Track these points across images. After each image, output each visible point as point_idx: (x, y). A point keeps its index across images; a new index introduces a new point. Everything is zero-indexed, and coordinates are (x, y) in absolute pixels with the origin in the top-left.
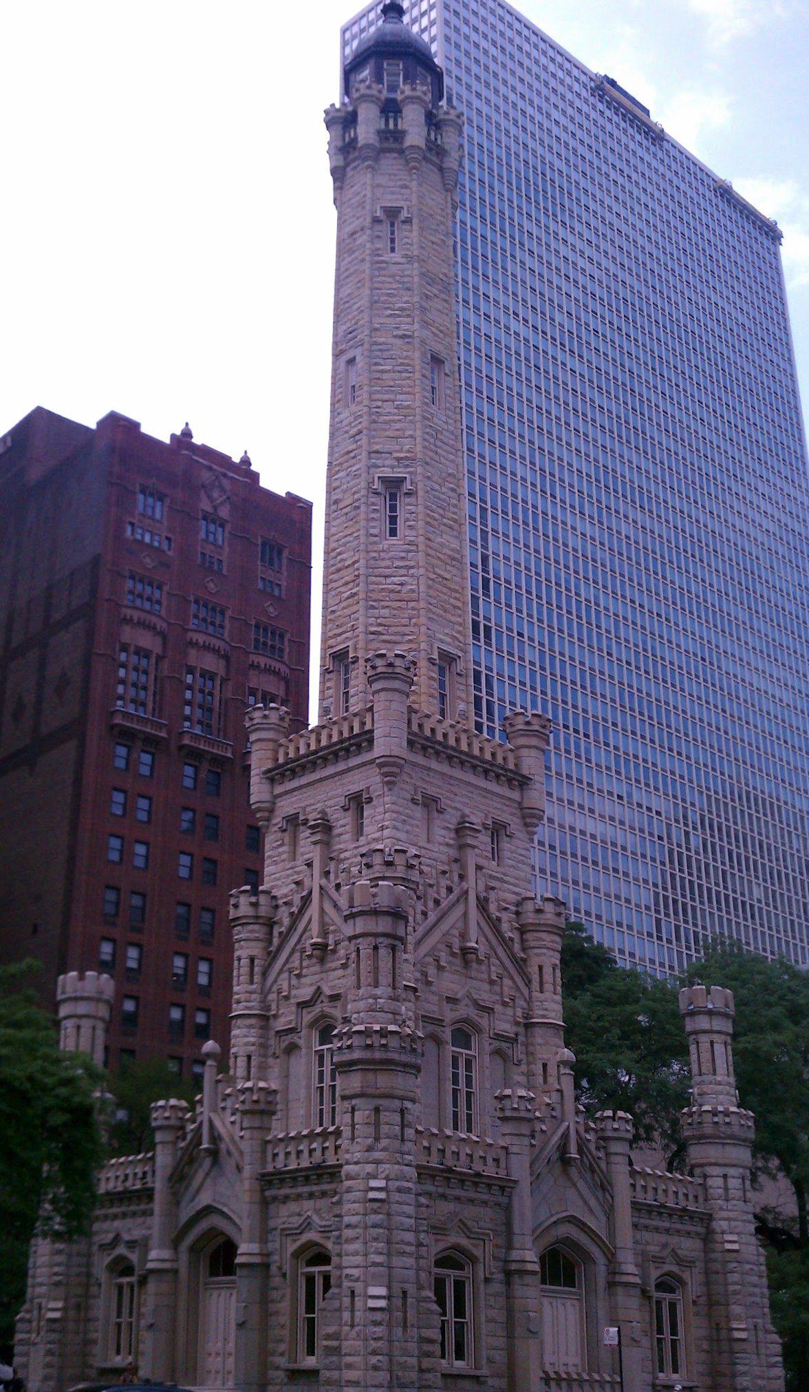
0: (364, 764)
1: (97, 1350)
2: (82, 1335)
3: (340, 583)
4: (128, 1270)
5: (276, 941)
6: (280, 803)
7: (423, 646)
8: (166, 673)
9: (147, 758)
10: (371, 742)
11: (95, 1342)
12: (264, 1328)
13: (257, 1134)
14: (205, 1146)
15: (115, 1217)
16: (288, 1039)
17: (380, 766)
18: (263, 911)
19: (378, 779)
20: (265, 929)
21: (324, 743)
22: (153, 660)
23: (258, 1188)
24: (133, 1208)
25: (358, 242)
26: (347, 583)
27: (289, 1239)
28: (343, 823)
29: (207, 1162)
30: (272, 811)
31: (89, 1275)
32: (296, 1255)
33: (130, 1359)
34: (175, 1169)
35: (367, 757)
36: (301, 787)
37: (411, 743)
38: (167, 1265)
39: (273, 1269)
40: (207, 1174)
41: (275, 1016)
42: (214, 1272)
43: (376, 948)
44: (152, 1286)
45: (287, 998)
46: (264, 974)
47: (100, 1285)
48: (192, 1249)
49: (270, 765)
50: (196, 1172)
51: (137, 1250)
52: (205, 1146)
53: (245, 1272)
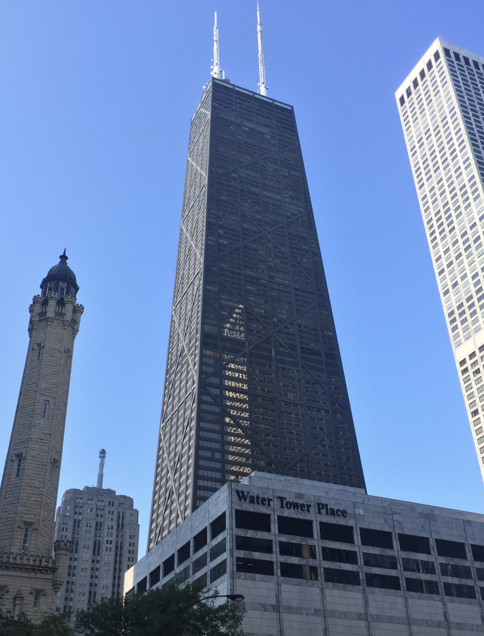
0: (44, 579)
3: (31, 492)
19: (51, 587)
25: (55, 354)
26: (35, 494)
28: (29, 599)
36: (7, 575)
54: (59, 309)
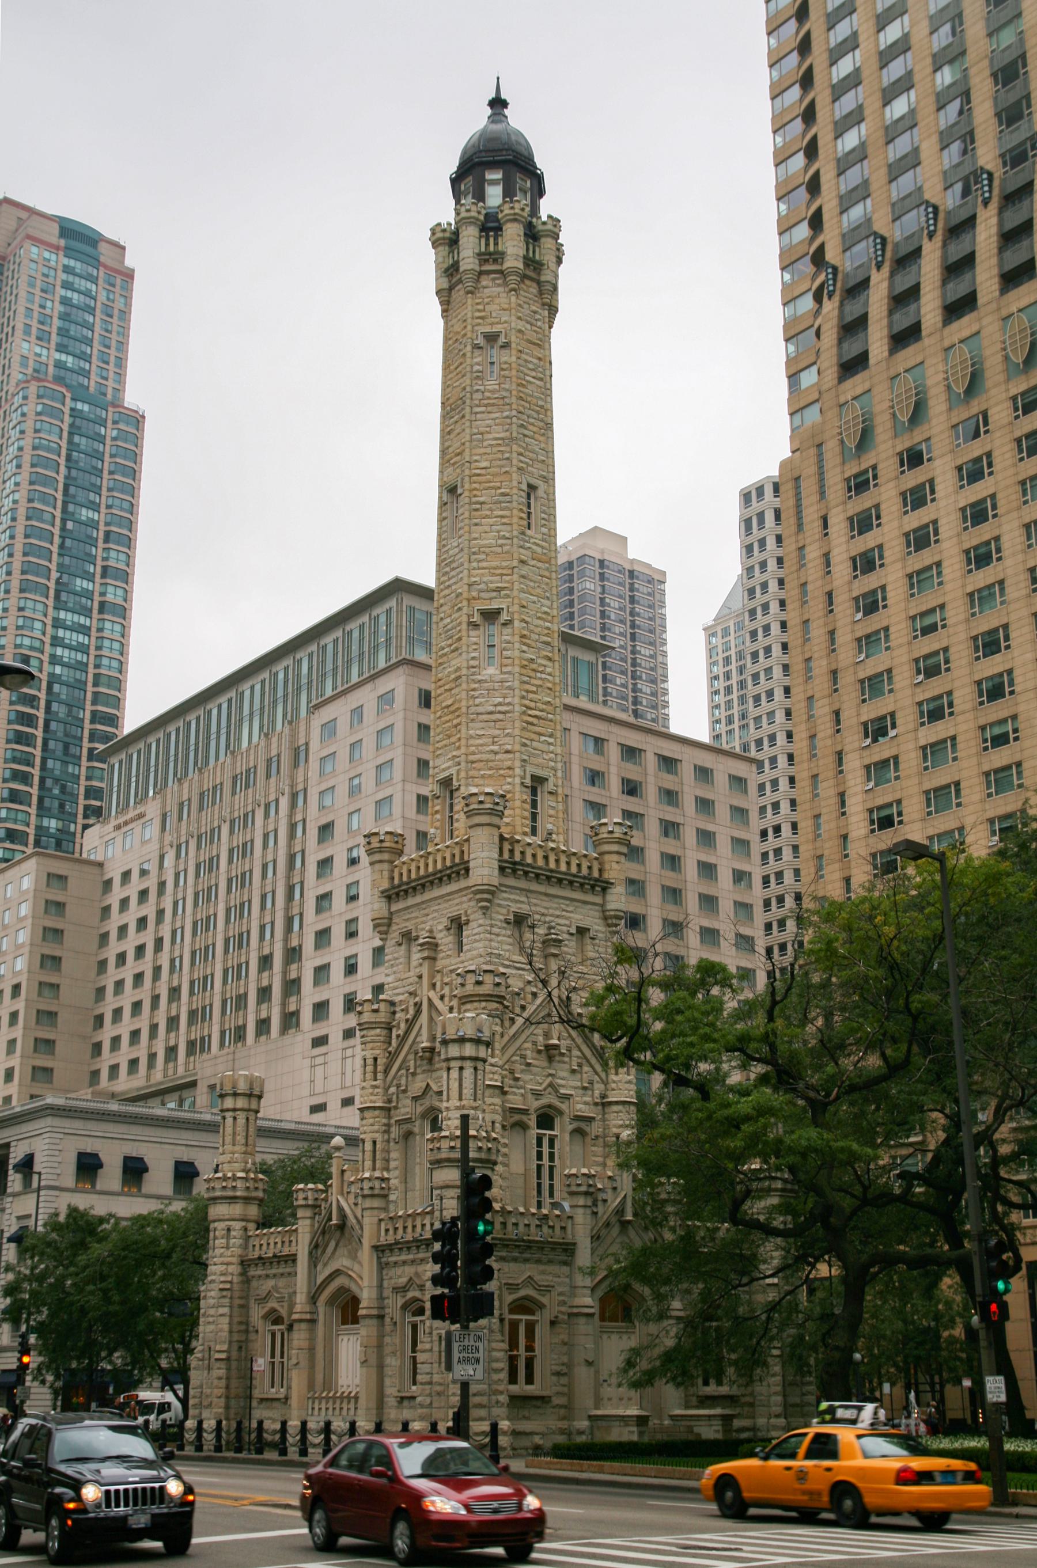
4: (278, 1320)
5: (394, 1043)
6: (395, 920)
7: (518, 771)
10: (467, 870)
12: (381, 1367)
14: (334, 1222)
16: (405, 1127)
17: (476, 893)
18: (382, 1017)
20: (384, 1032)
21: (430, 869)
28: (446, 940)
29: (338, 1234)
30: (389, 925)
31: (247, 1324)
32: (405, 1307)
35: (463, 883)
37: (502, 869)
39: (387, 1320)
41: (396, 1108)
42: (344, 1322)
43: (461, 1068)
45: (405, 1091)
46: (386, 1072)
49: (385, 885)
52: (334, 1222)
53: (368, 1322)
54: (487, 245)
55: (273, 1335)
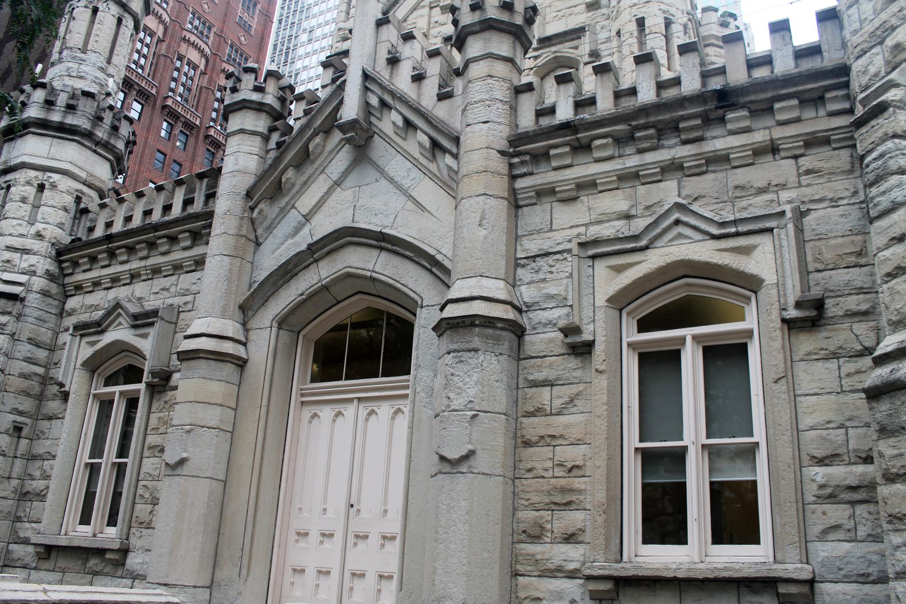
1: (47, 510)
2: (15, 482)
8: (163, 52)
9: (137, 107)
11: (41, 496)
13: (501, 69)
15: (115, 280)
22: (155, 40)
23: (503, 168)
24: (156, 260)
27: (601, 267)
29: (341, 161)
32: (620, 302)
33: (112, 531)
34: (261, 178)
38: (228, 347)
39: (544, 340)
40: (338, 183)
44: (189, 384)
47: (65, 396)
48: (282, 322)
50: (305, 185)
51: (152, 332)
55: (106, 405)
